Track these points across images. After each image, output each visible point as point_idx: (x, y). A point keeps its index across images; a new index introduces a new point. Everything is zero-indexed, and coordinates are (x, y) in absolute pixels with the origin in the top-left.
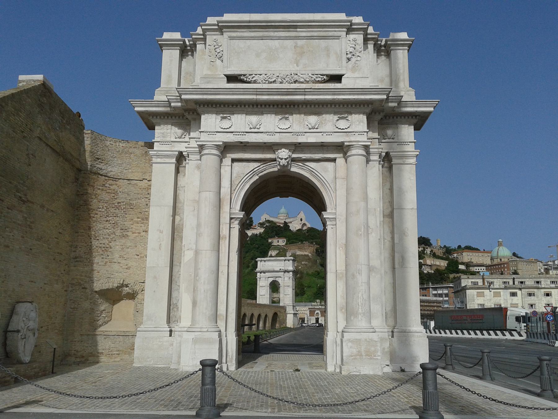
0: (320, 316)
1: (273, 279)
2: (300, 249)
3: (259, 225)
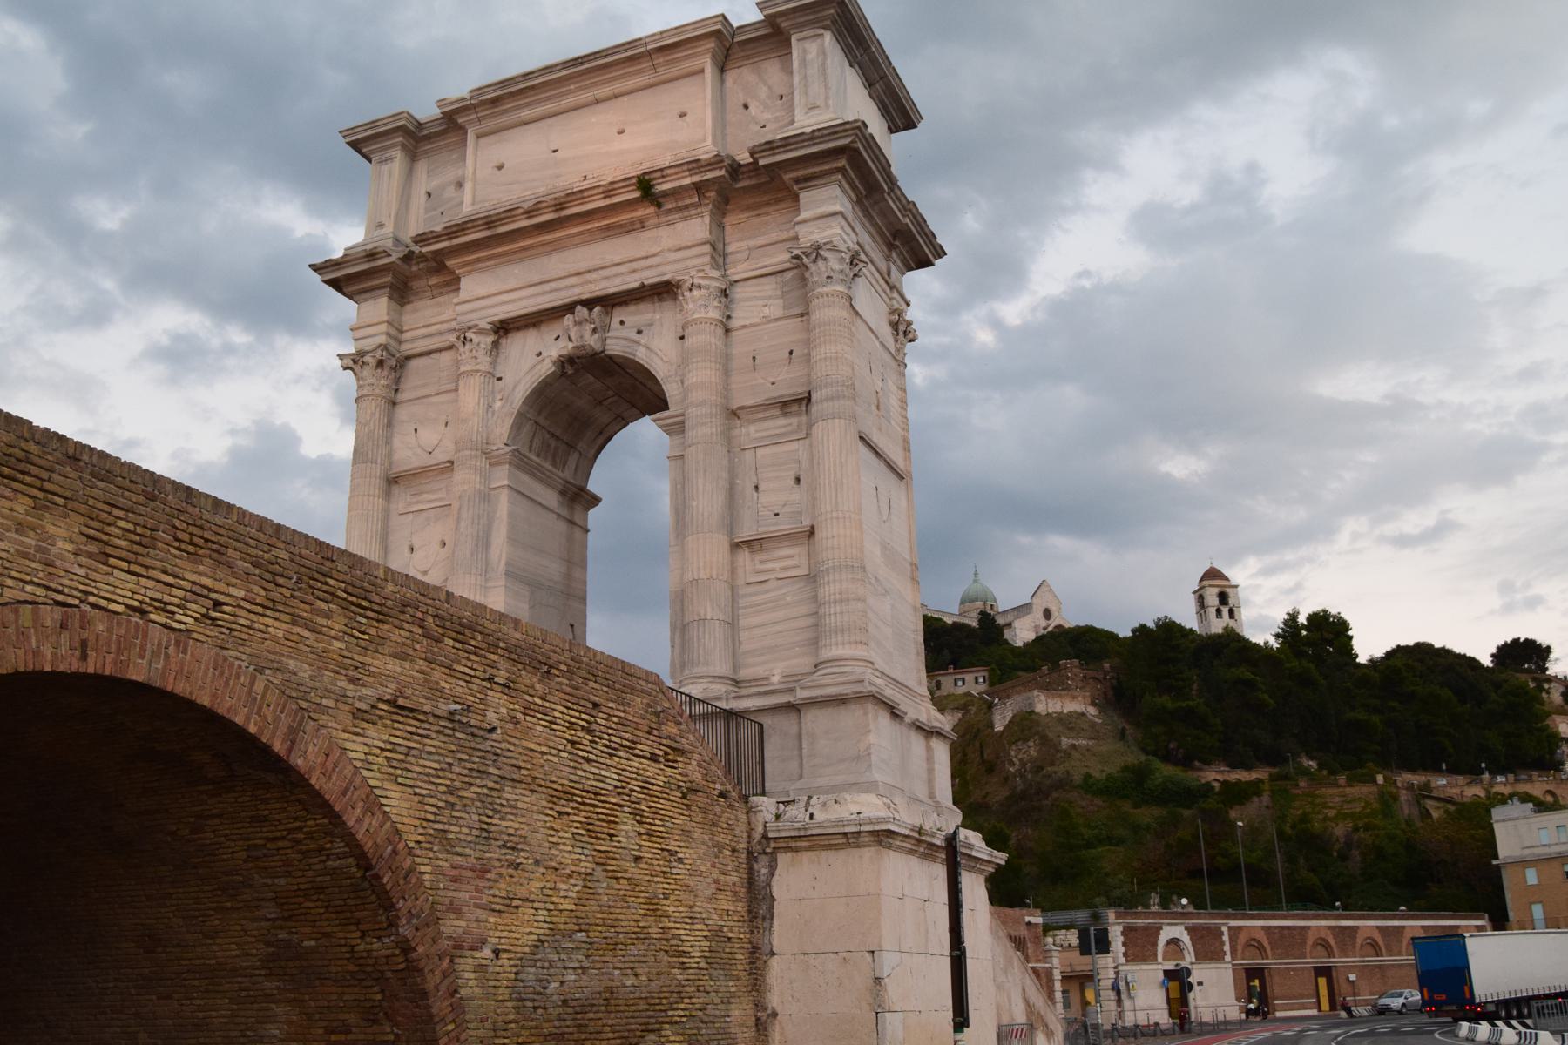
0: (1189, 958)
2: (1051, 687)
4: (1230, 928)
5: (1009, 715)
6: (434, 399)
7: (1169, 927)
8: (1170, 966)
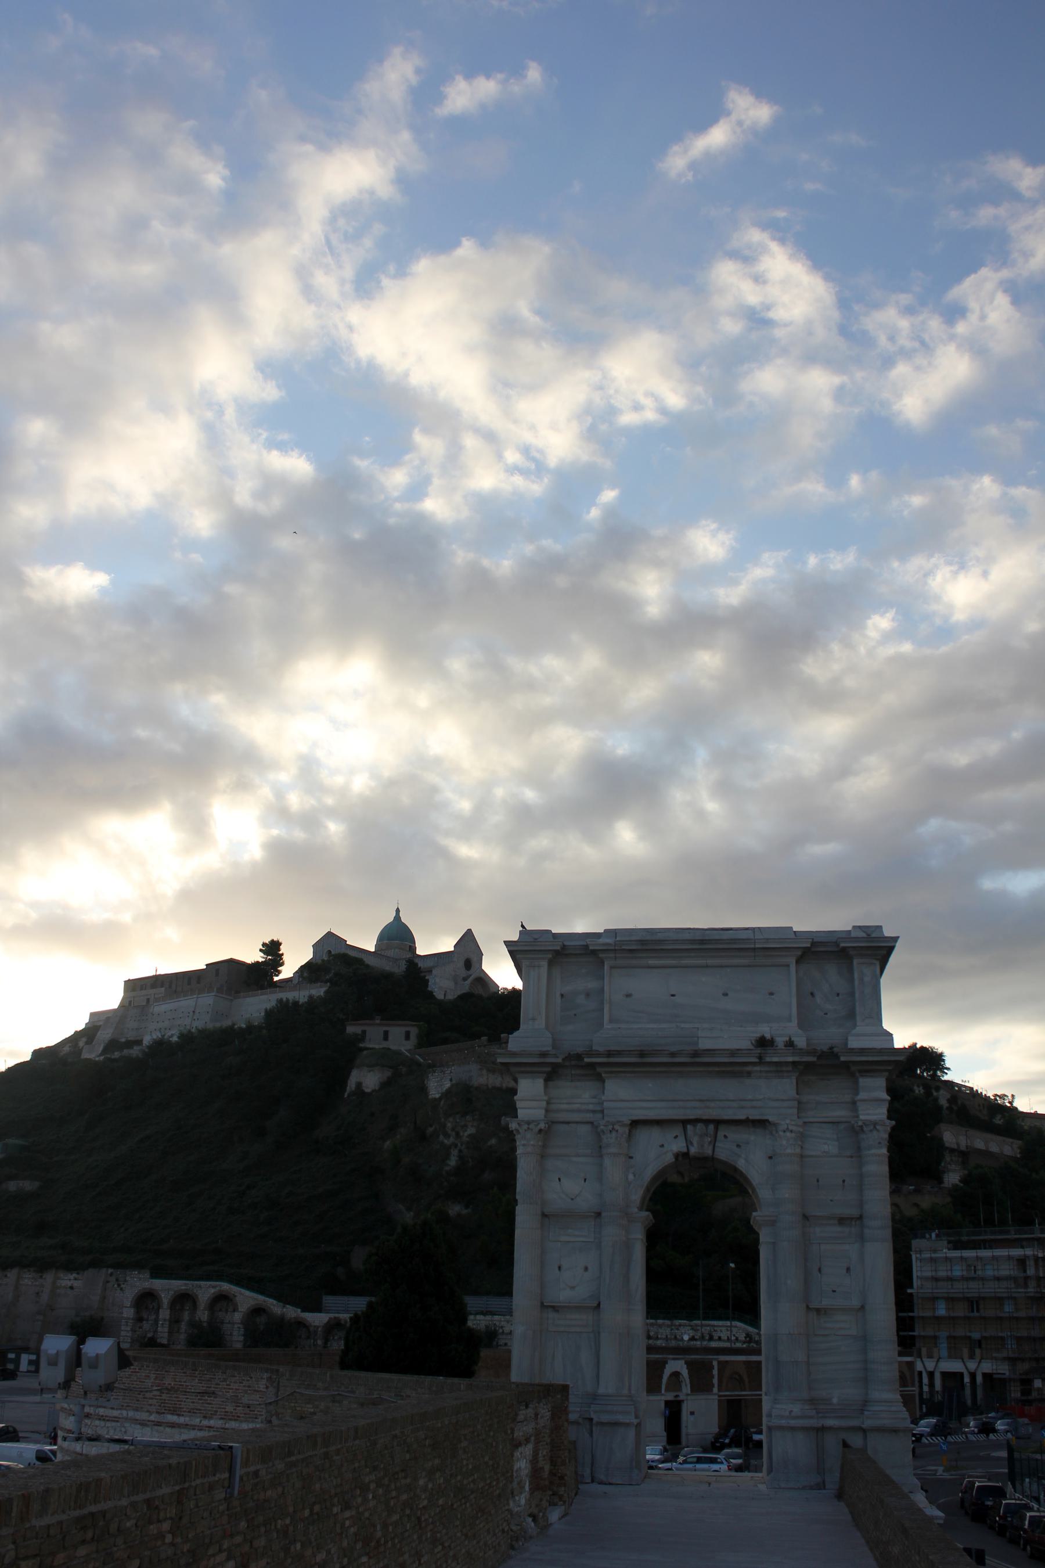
0: (686, 1388)
1: (678, 1146)
3: (305, 974)
4: (719, 1363)
5: (447, 1085)
6: (575, 1159)
7: (673, 1361)
8: (670, 1397)
